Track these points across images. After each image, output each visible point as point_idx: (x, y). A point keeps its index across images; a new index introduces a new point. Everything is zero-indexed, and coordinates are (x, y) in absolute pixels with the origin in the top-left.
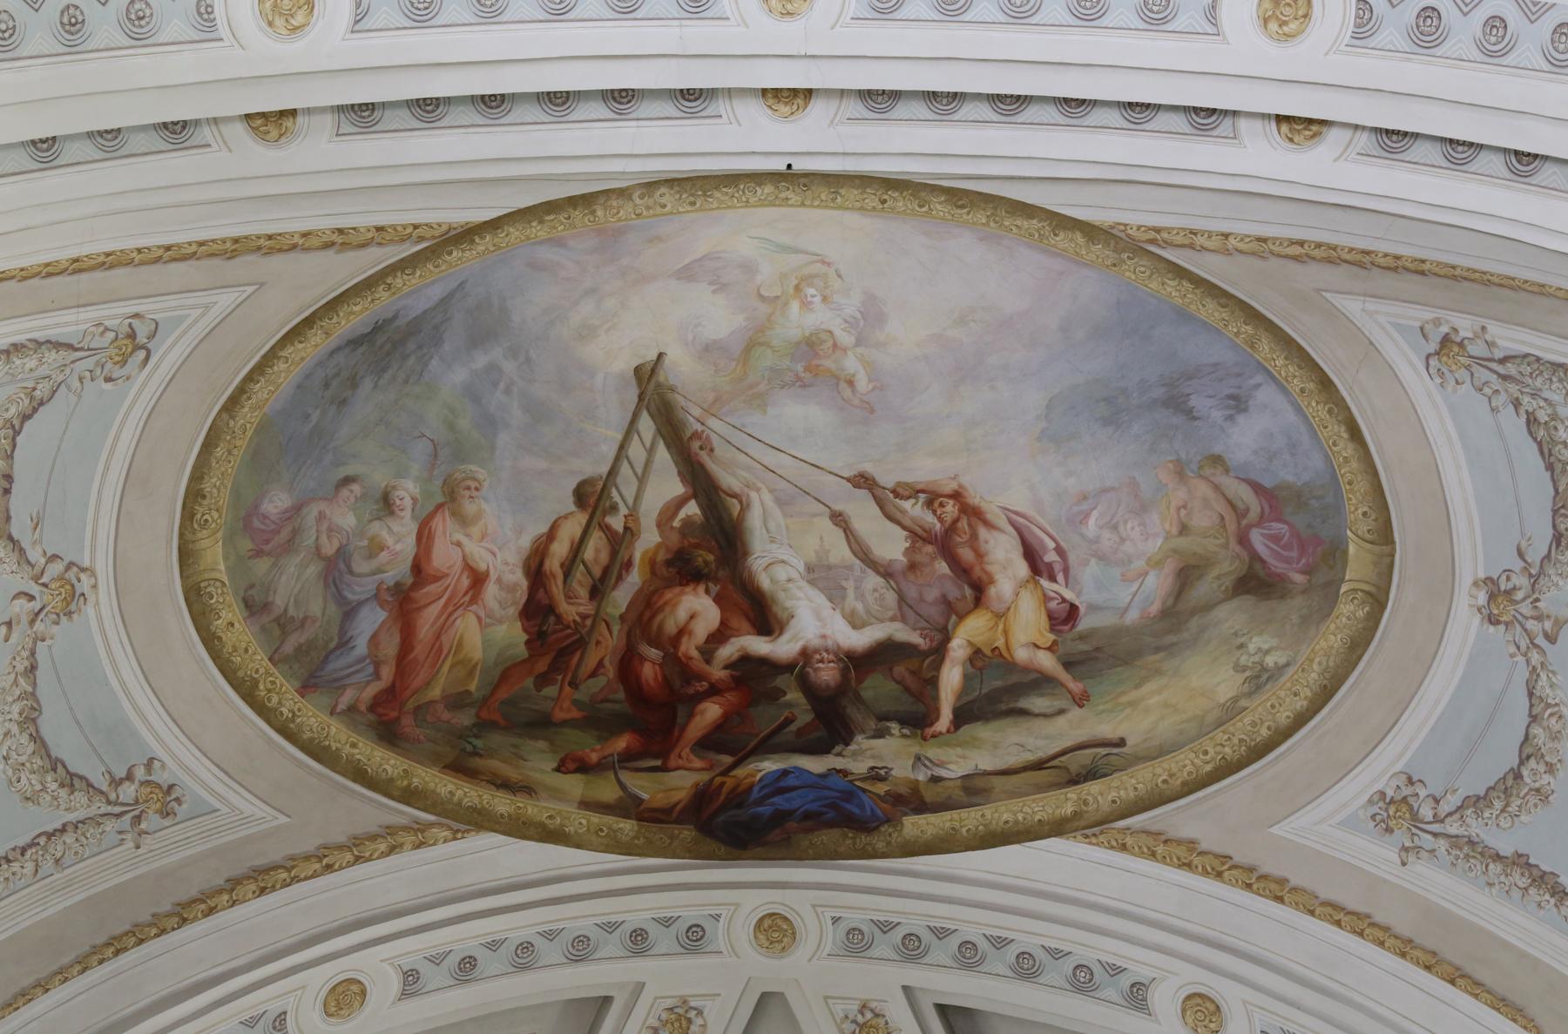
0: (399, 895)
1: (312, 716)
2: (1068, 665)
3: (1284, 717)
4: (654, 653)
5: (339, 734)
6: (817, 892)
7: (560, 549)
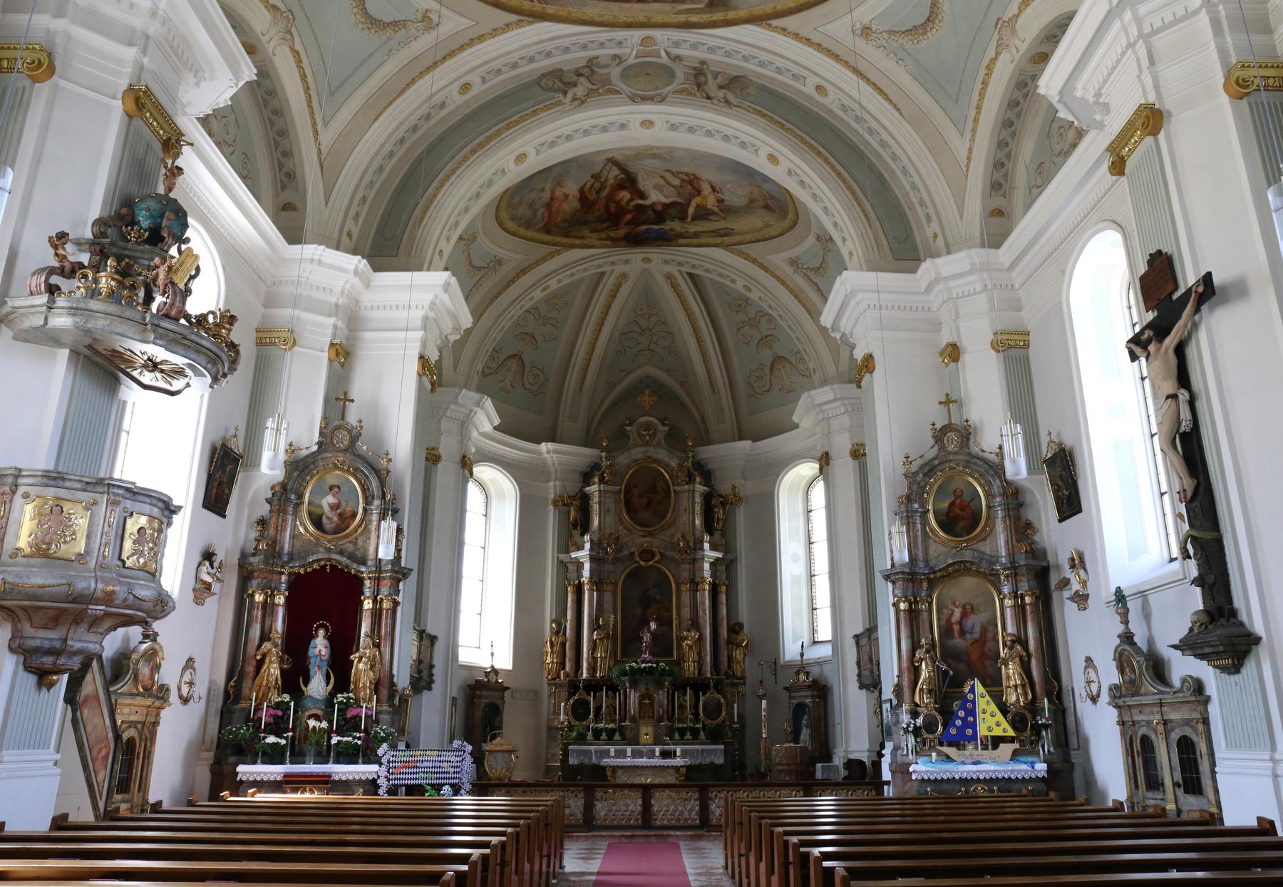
1: (530, 234)
7: (588, 186)
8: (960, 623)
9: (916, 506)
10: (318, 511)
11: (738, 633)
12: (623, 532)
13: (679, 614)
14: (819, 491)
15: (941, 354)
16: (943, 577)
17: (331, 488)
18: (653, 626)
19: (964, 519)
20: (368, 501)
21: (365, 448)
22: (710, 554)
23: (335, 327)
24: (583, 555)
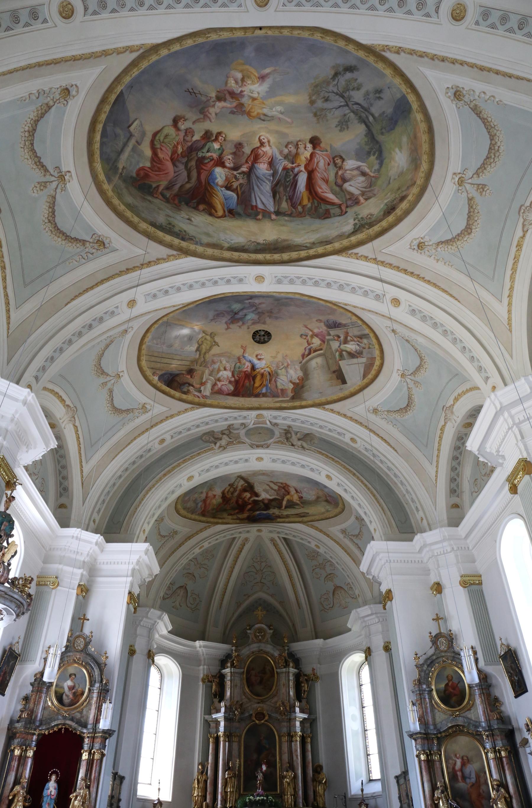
0: (207, 535)
1: (193, 516)
2: (301, 503)
3: (330, 516)
4: (241, 500)
5: (197, 517)
7: (227, 490)
8: (461, 770)
9: (424, 686)
10: (61, 691)
11: (319, 773)
12: (245, 700)
13: (281, 759)
14: (366, 672)
15: (431, 588)
16: (446, 736)
17: (70, 676)
18: (264, 768)
19: (455, 695)
20: (92, 685)
21: (93, 649)
22: (300, 716)
23: (82, 575)
24: (220, 716)
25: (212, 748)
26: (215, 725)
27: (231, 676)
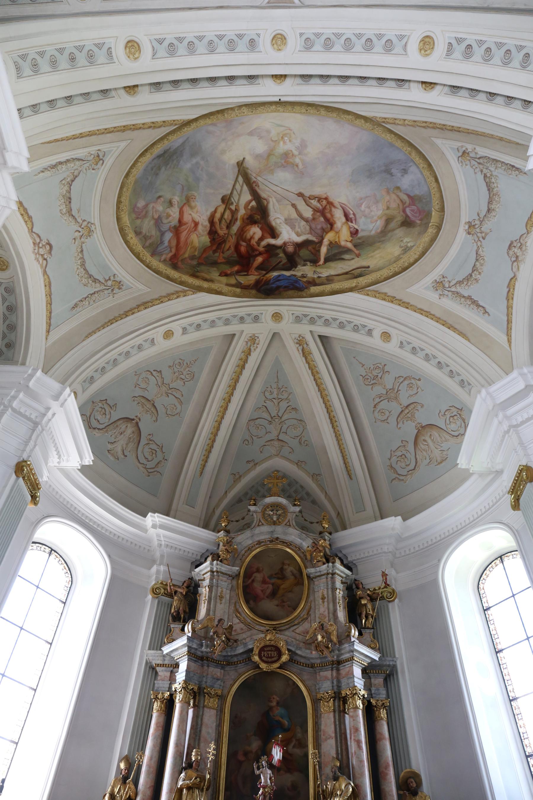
0: (180, 309)
1: (155, 263)
2: (355, 246)
3: (412, 260)
4: (244, 244)
5: (162, 267)
6: (288, 306)
7: (218, 215)
13: (317, 745)
18: (277, 754)
24: (178, 646)
25: (157, 724)
26: (168, 674)
27: (211, 579)
